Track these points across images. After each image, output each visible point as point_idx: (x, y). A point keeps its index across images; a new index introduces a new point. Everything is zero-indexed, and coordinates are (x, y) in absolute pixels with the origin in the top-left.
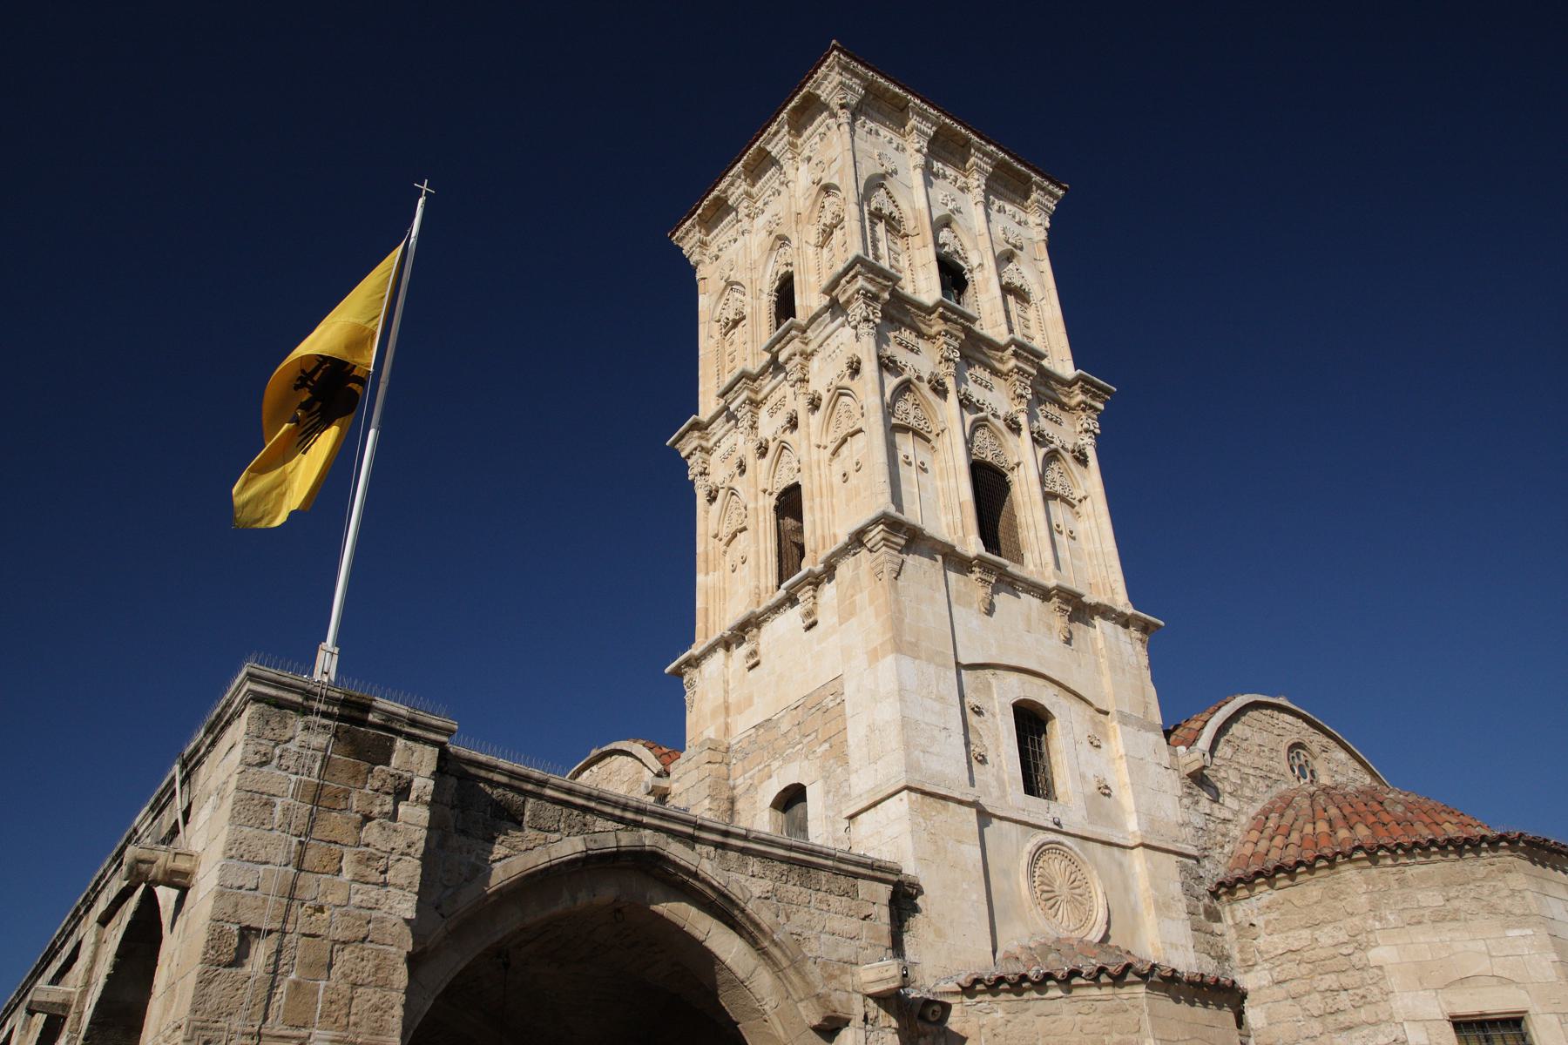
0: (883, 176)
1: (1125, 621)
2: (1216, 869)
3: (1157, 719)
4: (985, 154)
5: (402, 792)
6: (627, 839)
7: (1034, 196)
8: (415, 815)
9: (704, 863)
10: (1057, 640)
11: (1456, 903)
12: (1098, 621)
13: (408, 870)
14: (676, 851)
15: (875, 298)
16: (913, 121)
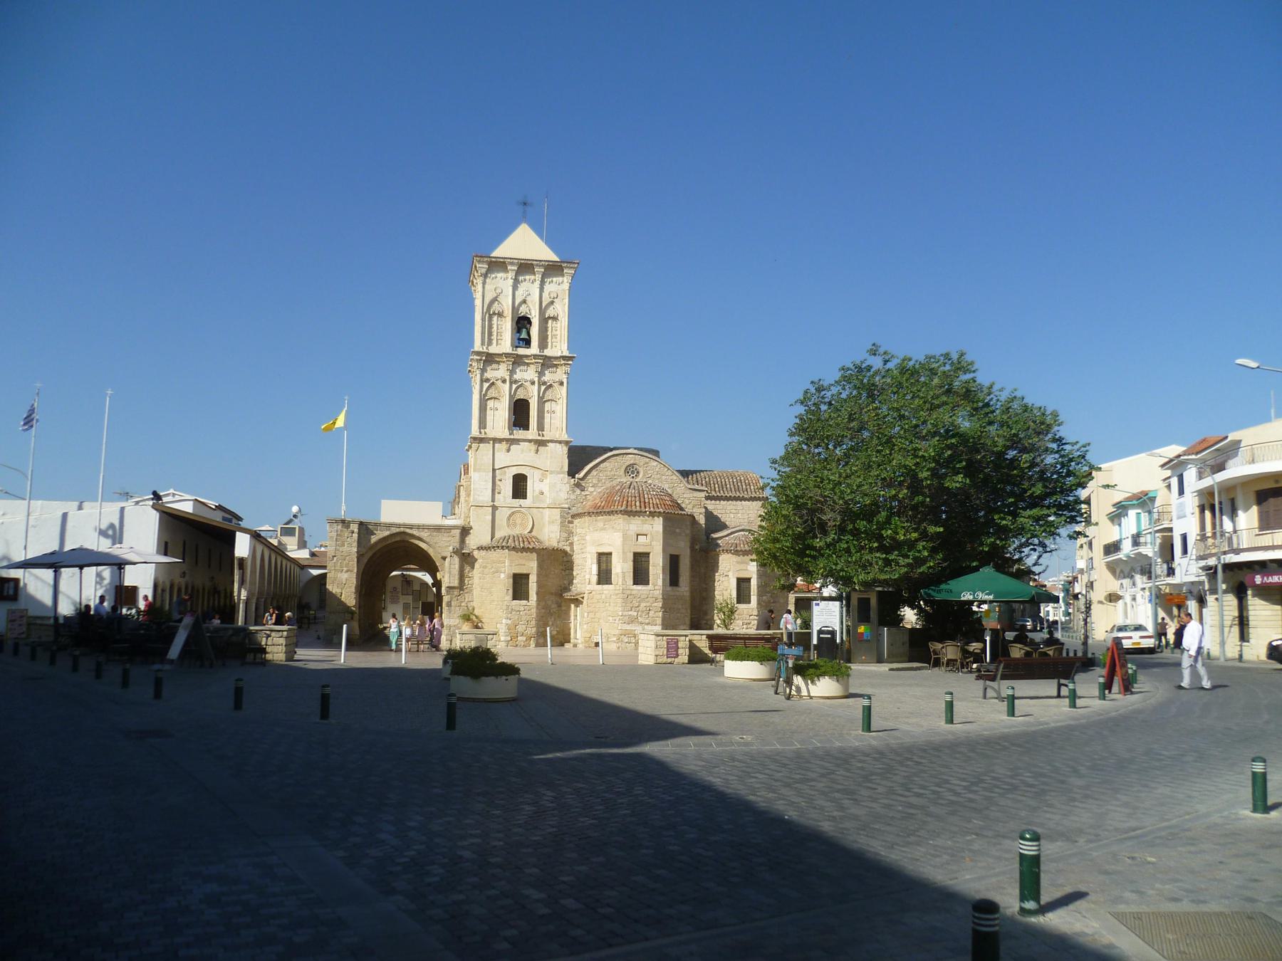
0: (497, 297)
1: (560, 442)
2: (574, 510)
3: (566, 469)
4: (540, 266)
5: (353, 532)
6: (398, 530)
7: (565, 271)
8: (355, 536)
9: (415, 532)
10: (533, 453)
11: (606, 526)
12: (550, 444)
13: (355, 544)
14: (408, 531)
15: (481, 360)
16: (509, 268)
